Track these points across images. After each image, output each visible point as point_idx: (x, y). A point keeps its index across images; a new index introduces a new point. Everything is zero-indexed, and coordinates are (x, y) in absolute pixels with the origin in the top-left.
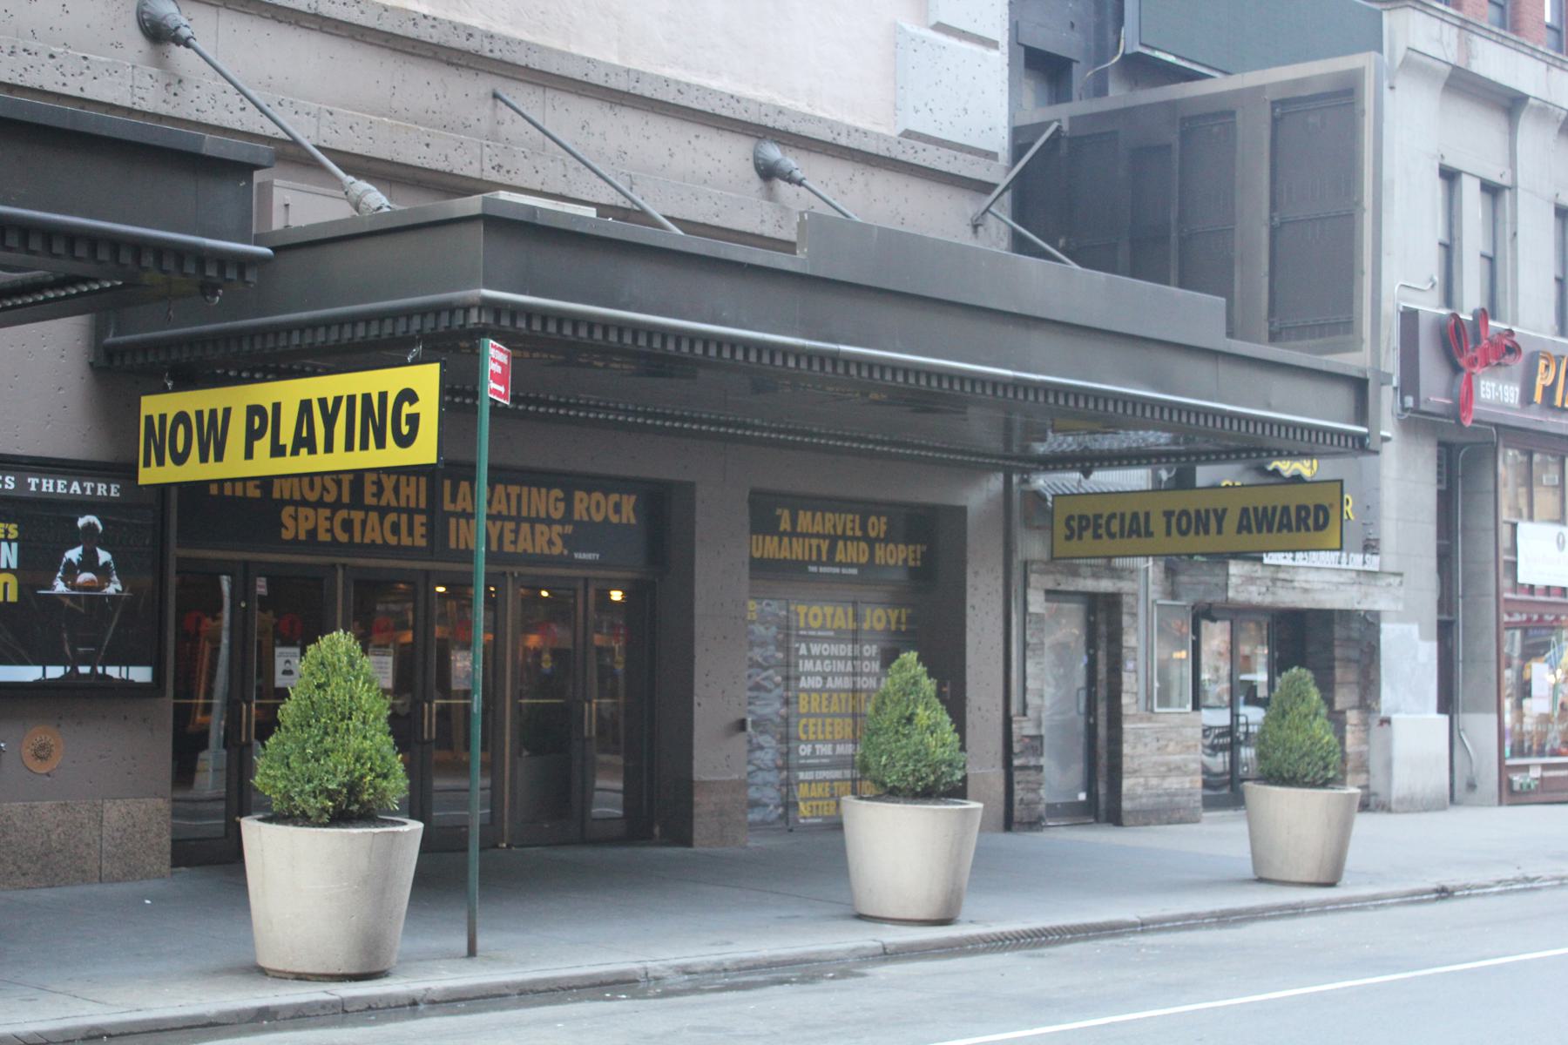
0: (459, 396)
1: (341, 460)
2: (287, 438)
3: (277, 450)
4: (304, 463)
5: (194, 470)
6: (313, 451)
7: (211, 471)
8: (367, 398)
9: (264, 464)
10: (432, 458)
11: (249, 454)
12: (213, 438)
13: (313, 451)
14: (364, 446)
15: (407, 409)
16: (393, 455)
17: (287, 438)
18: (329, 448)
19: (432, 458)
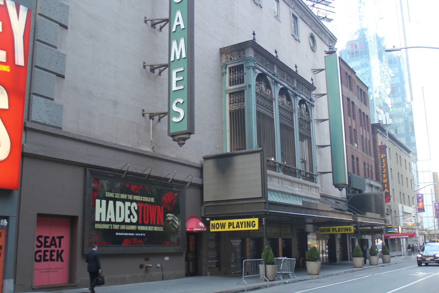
0: (260, 222)
1: (243, 229)
2: (235, 226)
3: (234, 227)
4: (238, 229)
5: (220, 230)
6: (239, 227)
7: (223, 230)
8: (247, 222)
9: (231, 229)
10: (257, 229)
11: (229, 228)
12: (223, 226)
13: (239, 227)
14: (247, 227)
15: (253, 223)
16: (251, 228)
17: (235, 226)
18: (242, 227)
19: (257, 229)
